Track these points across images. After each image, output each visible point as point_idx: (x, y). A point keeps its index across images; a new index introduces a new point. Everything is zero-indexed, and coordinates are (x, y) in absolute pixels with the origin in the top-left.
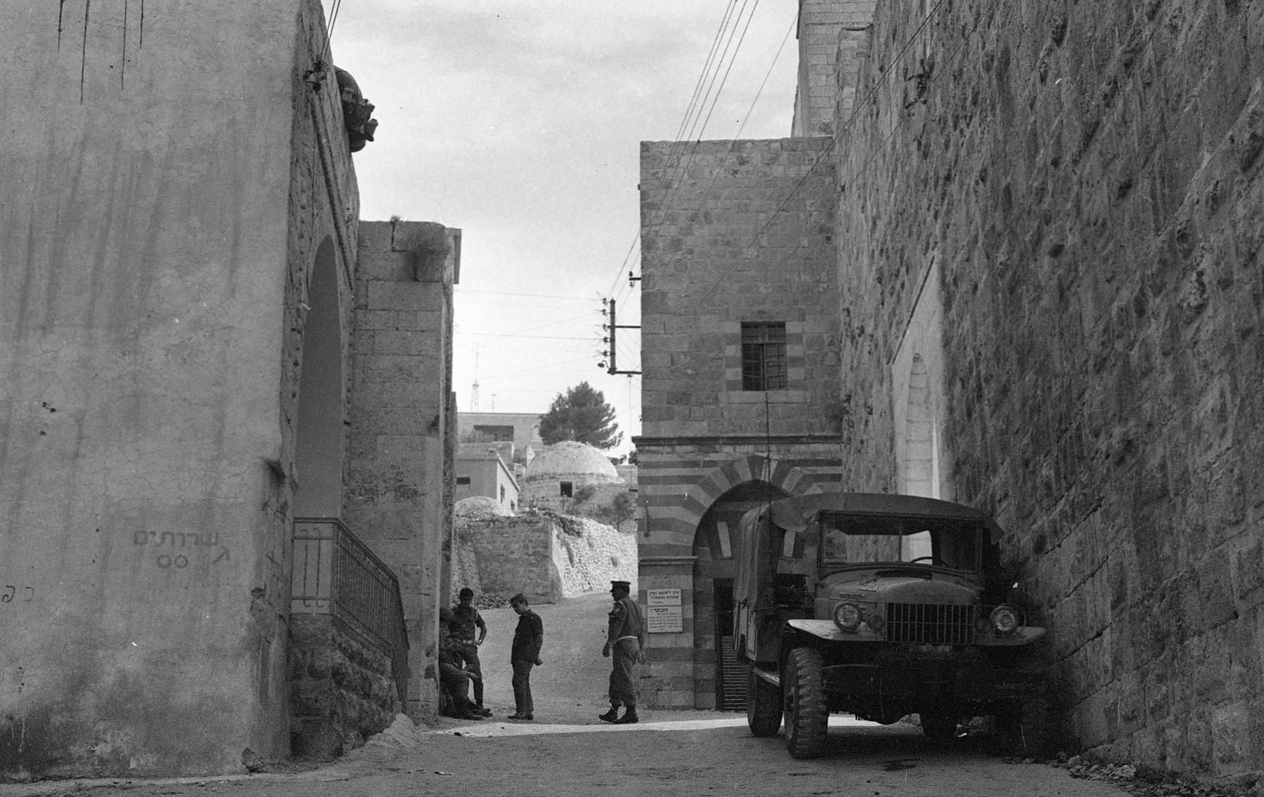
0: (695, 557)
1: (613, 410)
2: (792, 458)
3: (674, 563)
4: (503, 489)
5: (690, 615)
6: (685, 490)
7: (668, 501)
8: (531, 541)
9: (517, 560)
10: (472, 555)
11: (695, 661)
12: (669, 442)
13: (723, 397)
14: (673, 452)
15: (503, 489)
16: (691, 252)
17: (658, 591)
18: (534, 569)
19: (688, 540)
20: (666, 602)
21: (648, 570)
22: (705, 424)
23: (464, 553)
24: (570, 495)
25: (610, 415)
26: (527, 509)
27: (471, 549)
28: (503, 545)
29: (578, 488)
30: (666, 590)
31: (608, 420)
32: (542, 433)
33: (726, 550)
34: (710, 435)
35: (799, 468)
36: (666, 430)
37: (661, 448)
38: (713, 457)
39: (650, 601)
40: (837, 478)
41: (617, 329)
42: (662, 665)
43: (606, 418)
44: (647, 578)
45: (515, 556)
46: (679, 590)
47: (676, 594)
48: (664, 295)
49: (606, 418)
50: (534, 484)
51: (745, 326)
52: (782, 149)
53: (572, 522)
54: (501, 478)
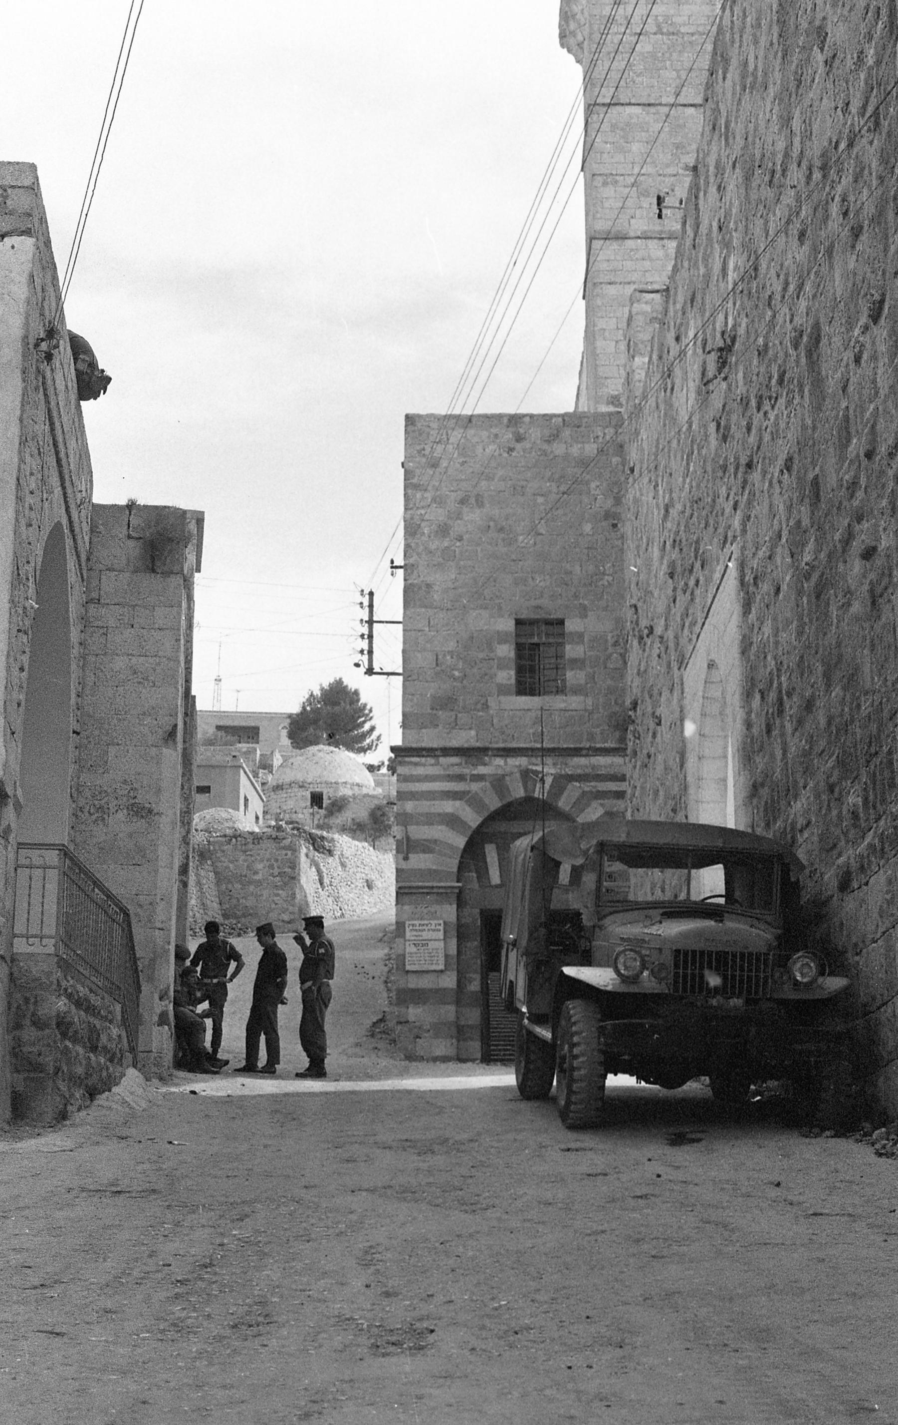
0: (460, 884)
1: (371, 711)
2: (570, 773)
3: (435, 890)
4: (246, 800)
5: (453, 950)
6: (448, 807)
7: (430, 819)
8: (277, 860)
9: (259, 881)
10: (212, 874)
11: (458, 1002)
12: (429, 752)
13: (492, 702)
14: (437, 764)
15: (246, 800)
16: (460, 539)
17: (417, 922)
18: (280, 892)
19: (453, 864)
20: (425, 935)
21: (406, 899)
22: (473, 733)
23: (202, 873)
24: (321, 807)
25: (367, 715)
26: (273, 823)
27: (211, 868)
28: (246, 864)
29: (329, 798)
30: (426, 922)
31: (364, 722)
32: (291, 736)
33: (495, 877)
34: (478, 744)
35: (578, 784)
36: (429, 739)
37: (423, 760)
38: (482, 770)
39: (408, 934)
40: (620, 795)
41: (375, 625)
42: (421, 1009)
43: (363, 719)
44: (406, 907)
45: (258, 877)
46: (441, 922)
48: (428, 586)
49: (363, 719)
50: (283, 794)
51: (519, 622)
52: (564, 424)
53: (322, 838)
54: (245, 787)
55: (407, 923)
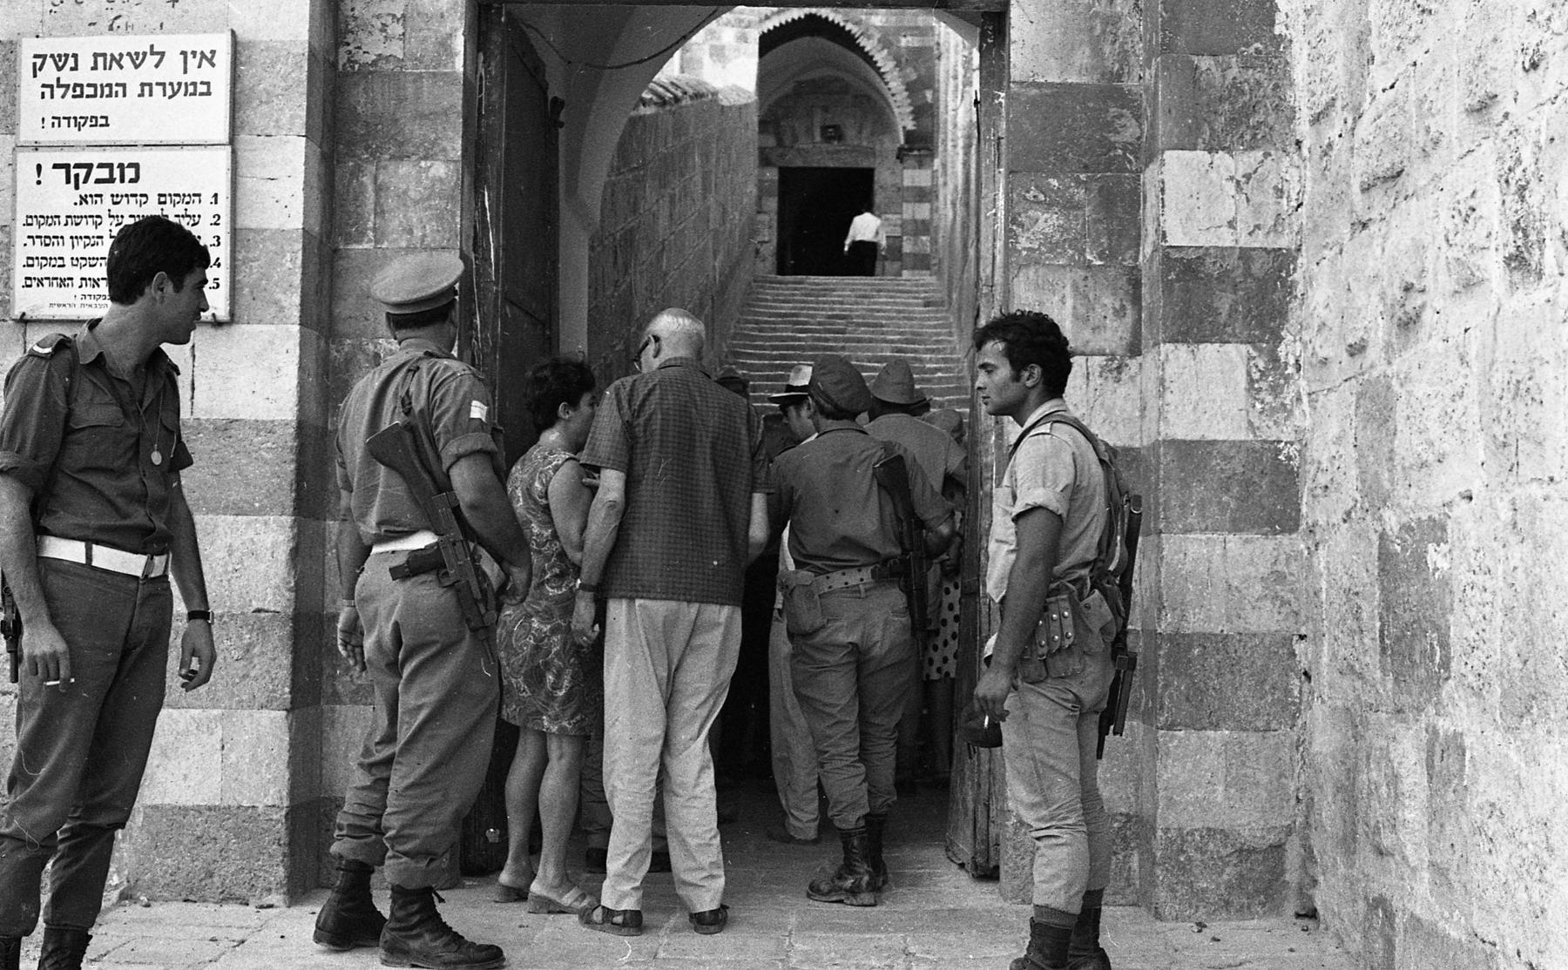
17: (85, 46)
30: (139, 44)
47: (195, 74)
55: (28, 50)
